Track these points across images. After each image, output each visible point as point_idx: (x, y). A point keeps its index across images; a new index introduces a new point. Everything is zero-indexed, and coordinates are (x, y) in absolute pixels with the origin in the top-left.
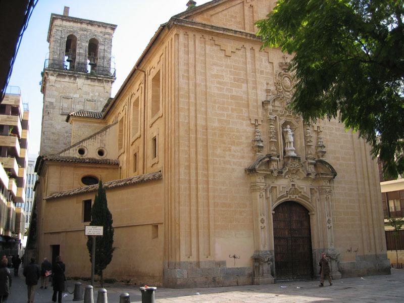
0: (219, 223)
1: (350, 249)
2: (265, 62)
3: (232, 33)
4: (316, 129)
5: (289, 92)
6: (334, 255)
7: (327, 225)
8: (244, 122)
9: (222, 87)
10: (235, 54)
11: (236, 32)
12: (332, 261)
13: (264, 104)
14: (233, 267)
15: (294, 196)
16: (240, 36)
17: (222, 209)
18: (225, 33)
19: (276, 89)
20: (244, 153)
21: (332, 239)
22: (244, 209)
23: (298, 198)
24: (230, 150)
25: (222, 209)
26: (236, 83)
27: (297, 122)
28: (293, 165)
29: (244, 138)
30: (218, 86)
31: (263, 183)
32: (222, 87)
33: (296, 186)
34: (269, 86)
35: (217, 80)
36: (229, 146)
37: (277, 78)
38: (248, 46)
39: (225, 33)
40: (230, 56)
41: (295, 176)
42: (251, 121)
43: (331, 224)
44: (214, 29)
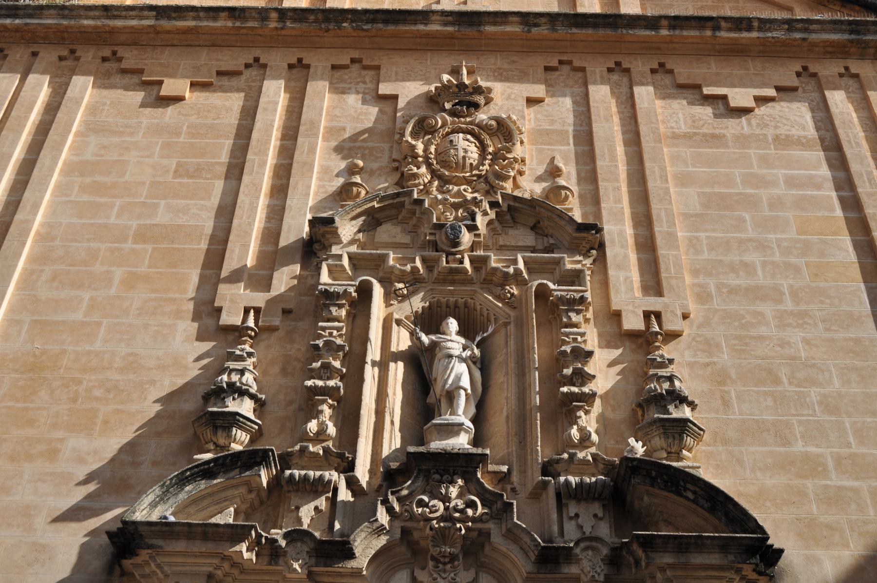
9: (103, 200)
30: (86, 198)
32: (103, 200)
35: (88, 180)
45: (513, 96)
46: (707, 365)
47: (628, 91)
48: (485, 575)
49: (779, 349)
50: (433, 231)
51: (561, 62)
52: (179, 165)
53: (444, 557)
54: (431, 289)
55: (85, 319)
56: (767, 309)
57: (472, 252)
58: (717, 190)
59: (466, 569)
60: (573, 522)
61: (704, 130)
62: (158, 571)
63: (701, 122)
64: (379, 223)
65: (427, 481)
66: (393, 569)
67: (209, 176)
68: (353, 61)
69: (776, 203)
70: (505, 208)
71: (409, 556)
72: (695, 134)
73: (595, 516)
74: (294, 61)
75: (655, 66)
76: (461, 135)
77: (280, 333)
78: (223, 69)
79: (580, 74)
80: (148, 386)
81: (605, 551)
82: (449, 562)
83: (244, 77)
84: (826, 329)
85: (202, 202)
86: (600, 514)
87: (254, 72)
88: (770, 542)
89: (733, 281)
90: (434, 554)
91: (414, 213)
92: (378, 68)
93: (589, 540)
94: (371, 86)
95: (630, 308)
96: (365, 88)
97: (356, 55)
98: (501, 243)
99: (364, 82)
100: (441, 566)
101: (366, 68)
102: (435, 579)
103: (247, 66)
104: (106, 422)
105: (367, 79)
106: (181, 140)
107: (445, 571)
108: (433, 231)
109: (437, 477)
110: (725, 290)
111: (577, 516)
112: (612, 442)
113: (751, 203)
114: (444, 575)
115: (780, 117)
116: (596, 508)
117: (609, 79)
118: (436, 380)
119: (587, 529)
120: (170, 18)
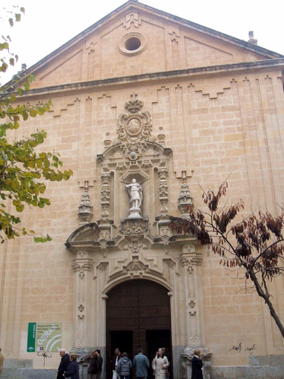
0: (29, 313)
1: (237, 346)
2: (106, 109)
3: (59, 89)
4: (179, 175)
5: (136, 136)
7: (188, 311)
8: (71, 187)
10: (67, 111)
11: (62, 87)
13: (100, 159)
14: (42, 368)
16: (69, 89)
17: (33, 296)
18: (50, 92)
19: (118, 138)
20: (67, 225)
21: (196, 331)
22: (60, 295)
23: (144, 274)
24: (49, 224)
25: (33, 296)
26: (65, 144)
27: (147, 172)
28: (131, 230)
29: (68, 207)
33: (139, 258)
34: (110, 136)
36: (50, 219)
37: (120, 123)
38: (83, 97)
39: (50, 92)
40: (59, 116)
41: (139, 245)
42: (79, 185)
43: (196, 308)
44: (37, 92)
45: (148, 103)
47: (181, 95)
49: (215, 178)
50: (128, 154)
51: (162, 87)
52: (63, 139)
54: (129, 171)
55: (49, 188)
56: (214, 166)
57: (138, 159)
58: (204, 129)
59: (140, 243)
60: (162, 231)
61: (202, 107)
63: (201, 104)
64: (115, 152)
66: (125, 244)
67: (70, 141)
68: (103, 95)
69: (220, 131)
70: (146, 145)
72: (199, 109)
73: (167, 229)
74: (87, 98)
75: (189, 85)
76: (134, 120)
77: (94, 187)
78: (69, 104)
79: (167, 91)
81: (168, 238)
83: (74, 106)
84: (228, 171)
85: (70, 150)
87: (77, 102)
89: (206, 158)
91: (123, 148)
92: (110, 97)
93: (165, 236)
94: (109, 103)
95: (178, 171)
96: (108, 105)
97: (104, 93)
98: (146, 155)
99: (107, 103)
100: (134, 243)
101: (107, 97)
103: (75, 101)
104: (59, 215)
105: (108, 101)
106: (62, 130)
107: (135, 244)
108: (128, 154)
109: (131, 224)
110: (203, 162)
111: (163, 230)
113: (212, 132)
115: (224, 99)
116: (167, 227)
117: (176, 91)
120: (52, 90)
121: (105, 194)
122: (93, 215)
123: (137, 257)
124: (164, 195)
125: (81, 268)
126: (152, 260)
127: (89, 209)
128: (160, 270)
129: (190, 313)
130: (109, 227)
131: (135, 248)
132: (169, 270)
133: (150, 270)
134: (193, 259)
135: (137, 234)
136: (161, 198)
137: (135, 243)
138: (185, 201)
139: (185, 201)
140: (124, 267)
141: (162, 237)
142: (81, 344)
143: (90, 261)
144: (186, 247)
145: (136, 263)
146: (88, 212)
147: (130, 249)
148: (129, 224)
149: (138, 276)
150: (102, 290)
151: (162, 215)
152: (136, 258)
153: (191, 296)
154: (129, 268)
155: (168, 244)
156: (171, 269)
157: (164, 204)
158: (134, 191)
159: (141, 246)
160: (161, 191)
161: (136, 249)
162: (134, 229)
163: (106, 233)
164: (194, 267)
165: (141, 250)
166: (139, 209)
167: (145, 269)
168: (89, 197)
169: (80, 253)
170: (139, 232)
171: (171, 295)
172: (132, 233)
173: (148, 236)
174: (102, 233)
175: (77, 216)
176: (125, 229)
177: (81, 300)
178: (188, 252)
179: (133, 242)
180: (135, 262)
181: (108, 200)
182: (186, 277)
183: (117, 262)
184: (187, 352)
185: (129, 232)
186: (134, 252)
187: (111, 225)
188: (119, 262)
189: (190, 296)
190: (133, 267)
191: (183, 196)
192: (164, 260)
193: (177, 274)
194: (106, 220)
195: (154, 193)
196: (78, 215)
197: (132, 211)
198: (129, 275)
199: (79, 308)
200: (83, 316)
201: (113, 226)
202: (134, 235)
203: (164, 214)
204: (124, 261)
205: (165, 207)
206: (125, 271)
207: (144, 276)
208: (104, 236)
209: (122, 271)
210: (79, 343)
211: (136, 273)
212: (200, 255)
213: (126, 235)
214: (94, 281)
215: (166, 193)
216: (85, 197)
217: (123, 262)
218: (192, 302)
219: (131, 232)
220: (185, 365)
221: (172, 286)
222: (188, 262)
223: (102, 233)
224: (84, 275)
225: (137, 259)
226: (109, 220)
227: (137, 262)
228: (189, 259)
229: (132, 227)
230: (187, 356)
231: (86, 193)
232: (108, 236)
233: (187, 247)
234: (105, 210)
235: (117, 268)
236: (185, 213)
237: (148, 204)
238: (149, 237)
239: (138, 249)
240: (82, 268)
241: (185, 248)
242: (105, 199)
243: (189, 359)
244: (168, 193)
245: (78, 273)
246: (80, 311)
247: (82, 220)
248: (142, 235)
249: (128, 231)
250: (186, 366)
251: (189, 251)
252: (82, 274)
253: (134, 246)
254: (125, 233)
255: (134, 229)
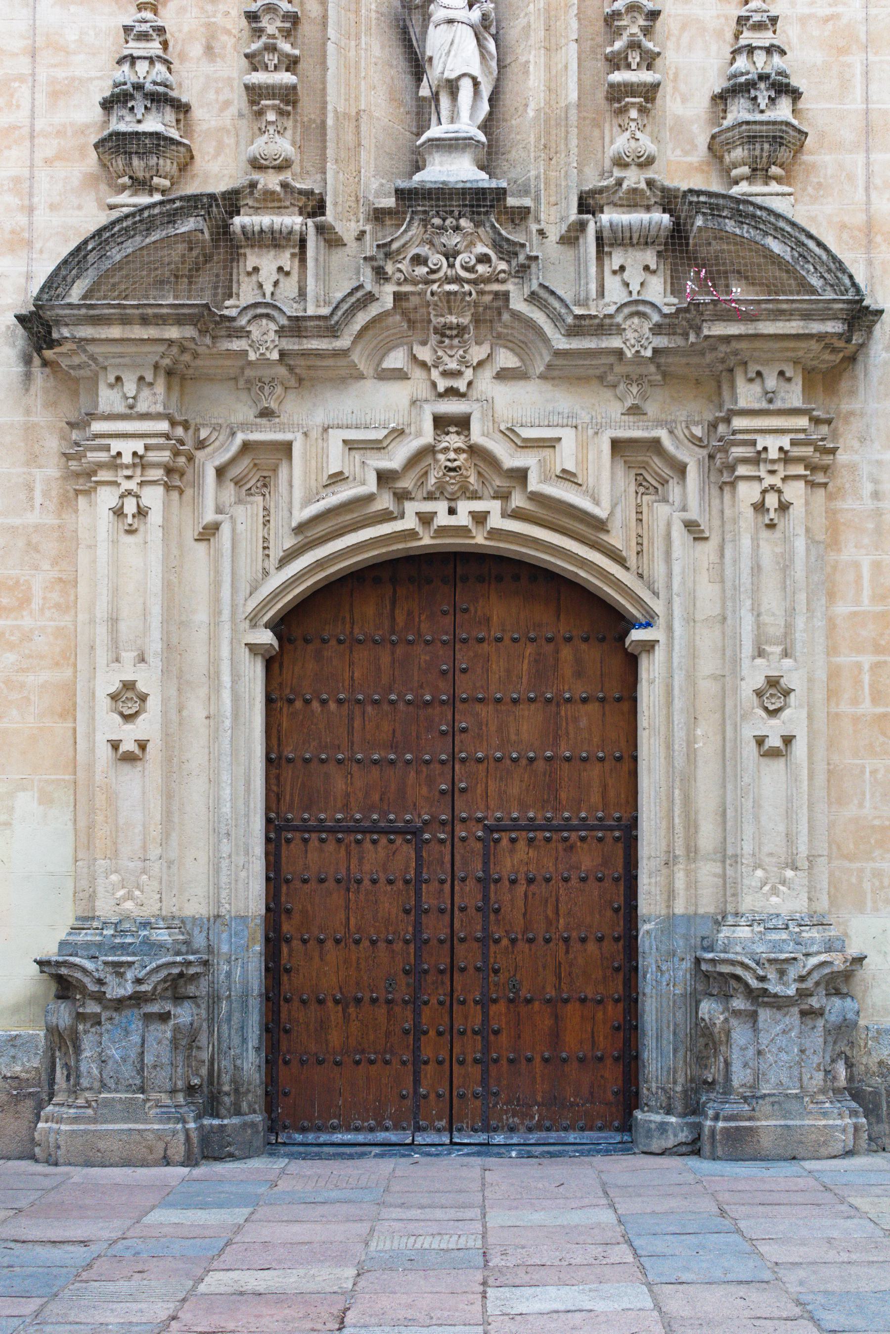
6: (781, 966)
7: (749, 732)
12: (764, 1015)
15: (465, 507)
21: (790, 838)
23: (496, 521)
28: (436, 259)
31: (145, 416)
33: (475, 426)
41: (478, 353)
46: (827, 20)
48: (502, 350)
53: (451, 328)
60: (618, 278)
62: (91, 362)
65: (425, 226)
71: (405, 325)
73: (646, 268)
80: (17, 84)
82: (456, 336)
86: (653, 267)
88: (865, 303)
90: (439, 326)
100: (447, 341)
102: (439, 358)
107: (451, 347)
109: (437, 221)
111: (622, 268)
112: (678, 152)
114: (449, 352)
118: (431, 59)
119: (635, 287)
121: (271, 25)
122: (192, 157)
123: (463, 423)
124: (634, 58)
125: (127, 467)
126: (551, 444)
127: (170, 115)
128: (597, 503)
129: (760, 741)
130: (297, 228)
131: (453, 365)
132: (639, 506)
133: (535, 497)
134: (793, 443)
135: (468, 282)
136: (617, 77)
137: (451, 337)
138: (762, 107)
139: (762, 107)
140: (384, 478)
141: (619, 310)
142: (130, 897)
143: (179, 431)
144: (754, 375)
145: (452, 455)
146: (166, 134)
147: (418, 374)
148: (425, 222)
149: (463, 531)
150: (252, 604)
151: (619, 183)
152: (452, 429)
153: (769, 649)
154: (407, 483)
155: (649, 353)
156: (653, 497)
157: (634, 113)
158: (450, 21)
159: (483, 356)
160: (618, 32)
161: (458, 374)
162: (451, 255)
163: (280, 269)
164: (795, 492)
165: (486, 384)
166: (482, 138)
167: (503, 496)
168: (165, 45)
169: (118, 379)
170: (481, 269)
171: (649, 646)
172: (441, 274)
173: (533, 298)
174: (256, 270)
175: (94, 155)
176: (398, 251)
177: (128, 656)
178: (764, 405)
179: (442, 332)
180: (446, 449)
181: (292, 64)
182: (746, 542)
183: (341, 443)
184: (738, 949)
185: (422, 270)
186: (441, 389)
187: (310, 222)
188: (350, 445)
189: (760, 653)
190: (432, 481)
191: (748, 73)
192: (616, 444)
193: (690, 526)
194: (278, 189)
195: (574, 46)
196: (96, 146)
197: (438, 144)
198: (410, 522)
199: (114, 697)
200: (143, 745)
201: (321, 229)
202: (454, 287)
203: (634, 178)
204: (380, 441)
205: (638, 135)
206: (385, 502)
207: (495, 533)
208: (268, 288)
209: (369, 498)
210: (121, 893)
211: (452, 511)
212: (824, 429)
213: (399, 284)
214: (202, 547)
215: (650, 45)
216: (143, 37)
217: (376, 446)
218: (773, 682)
219: (433, 272)
220: (722, 1018)
221: (656, 594)
222: (765, 461)
223: (256, 270)
224: (142, 513)
225: (458, 433)
226: (301, 192)
227: (457, 450)
228: (773, 444)
229: (444, 240)
230: (739, 971)
231: (148, 15)
232: (289, 287)
233: (759, 374)
234: (271, 129)
235: (337, 478)
236: (749, 179)
237: (531, 113)
238: (543, 306)
239: (469, 374)
240: (134, 465)
241: (751, 380)
242: (271, 59)
243: (747, 985)
244: (657, 50)
245: (107, 498)
246: (122, 715)
247: (126, 180)
248: (496, 294)
249: (418, 260)
250: (726, 1020)
251: (770, 401)
252: (130, 507)
253: (446, 359)
254: (398, 275)
255: (451, 255)
